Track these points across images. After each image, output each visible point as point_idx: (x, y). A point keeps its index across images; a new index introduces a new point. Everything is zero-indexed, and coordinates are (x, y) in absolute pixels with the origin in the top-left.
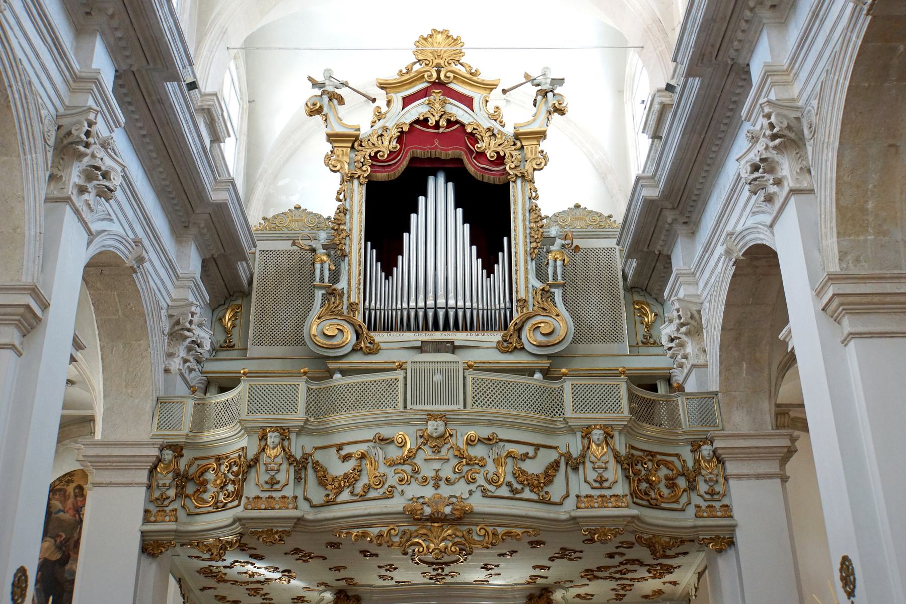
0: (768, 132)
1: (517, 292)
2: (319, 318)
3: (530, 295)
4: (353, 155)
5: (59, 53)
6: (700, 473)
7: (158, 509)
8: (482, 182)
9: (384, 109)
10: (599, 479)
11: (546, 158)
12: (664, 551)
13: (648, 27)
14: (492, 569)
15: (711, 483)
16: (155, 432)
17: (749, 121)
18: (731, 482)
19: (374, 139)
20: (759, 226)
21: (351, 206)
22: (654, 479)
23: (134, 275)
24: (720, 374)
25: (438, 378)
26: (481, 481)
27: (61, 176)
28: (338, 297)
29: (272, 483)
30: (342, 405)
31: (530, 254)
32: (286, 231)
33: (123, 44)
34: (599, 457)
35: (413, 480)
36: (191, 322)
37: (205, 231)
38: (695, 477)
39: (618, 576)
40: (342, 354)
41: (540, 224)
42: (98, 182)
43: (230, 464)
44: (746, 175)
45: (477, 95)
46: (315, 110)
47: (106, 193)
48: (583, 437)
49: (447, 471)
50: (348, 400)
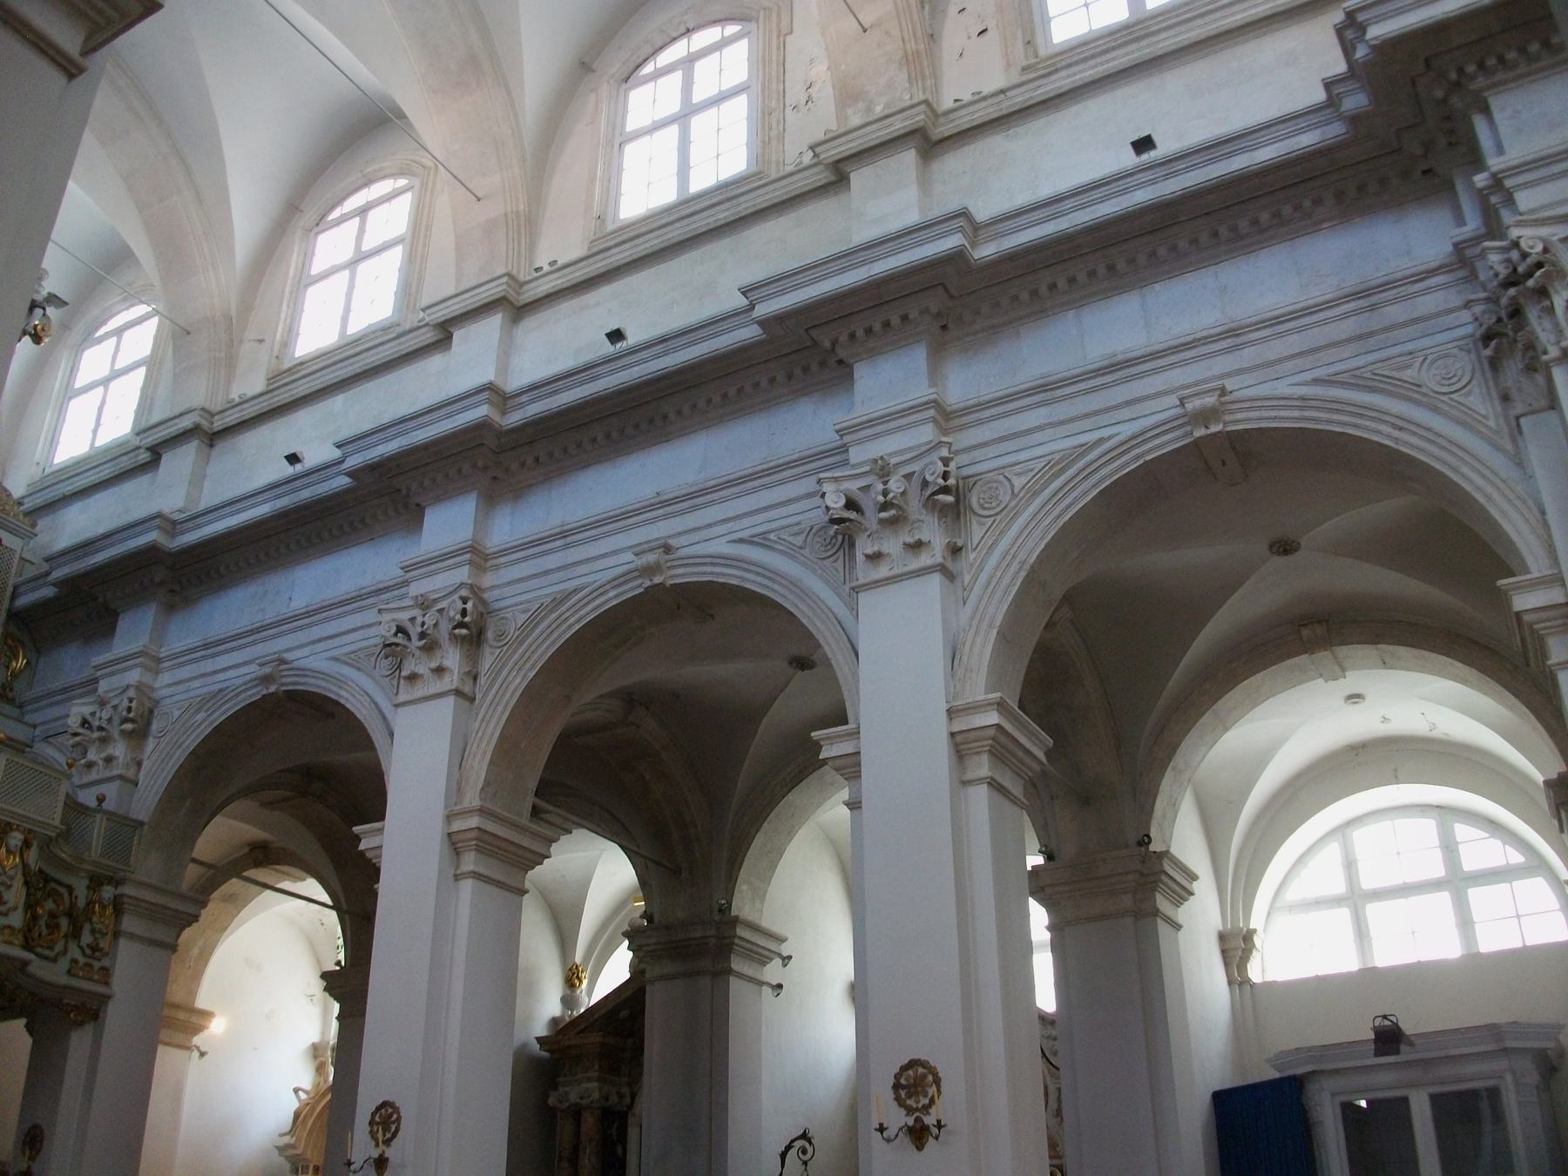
15: (98, 936)
18: (122, 942)
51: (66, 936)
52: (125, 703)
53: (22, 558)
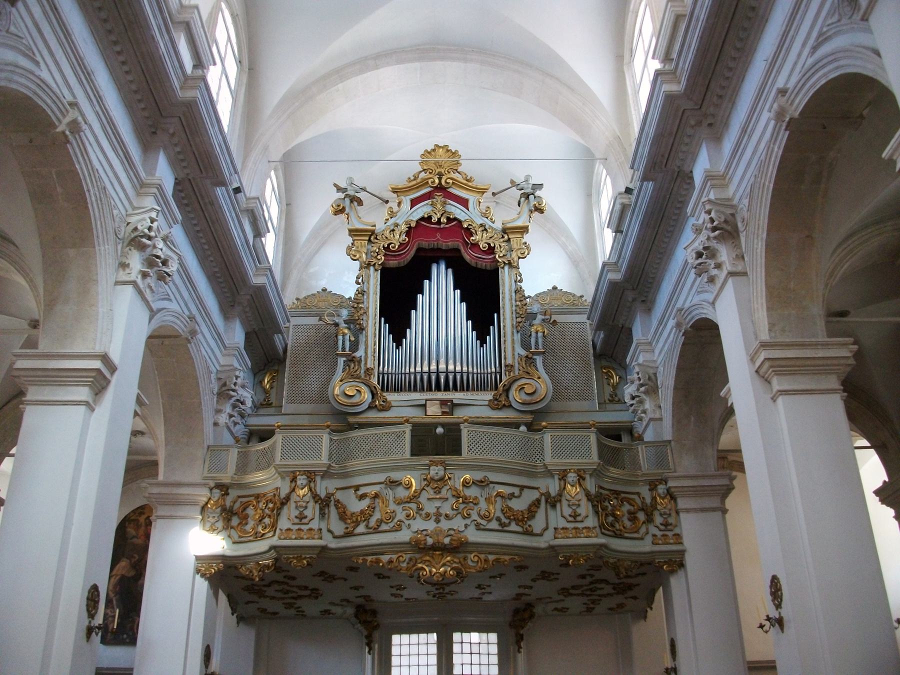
0: (709, 225)
1: (505, 358)
2: (341, 381)
3: (516, 361)
5: (129, 164)
6: (656, 508)
9: (396, 208)
10: (573, 514)
11: (528, 248)
12: (626, 573)
13: (610, 143)
14: (484, 588)
16: (206, 474)
17: (693, 217)
18: (682, 515)
19: (387, 233)
20: (704, 303)
21: (368, 289)
22: (618, 513)
23: (189, 345)
25: (440, 430)
26: (475, 516)
27: (129, 264)
28: (357, 363)
29: (301, 517)
32: (315, 309)
33: (181, 157)
34: (573, 496)
35: (418, 516)
36: (235, 384)
37: (247, 309)
38: (652, 511)
39: (588, 593)
41: (524, 303)
42: (159, 269)
43: (267, 501)
44: (692, 260)
45: (472, 198)
46: (339, 211)
47: (162, 277)
48: (560, 479)
49: (446, 509)
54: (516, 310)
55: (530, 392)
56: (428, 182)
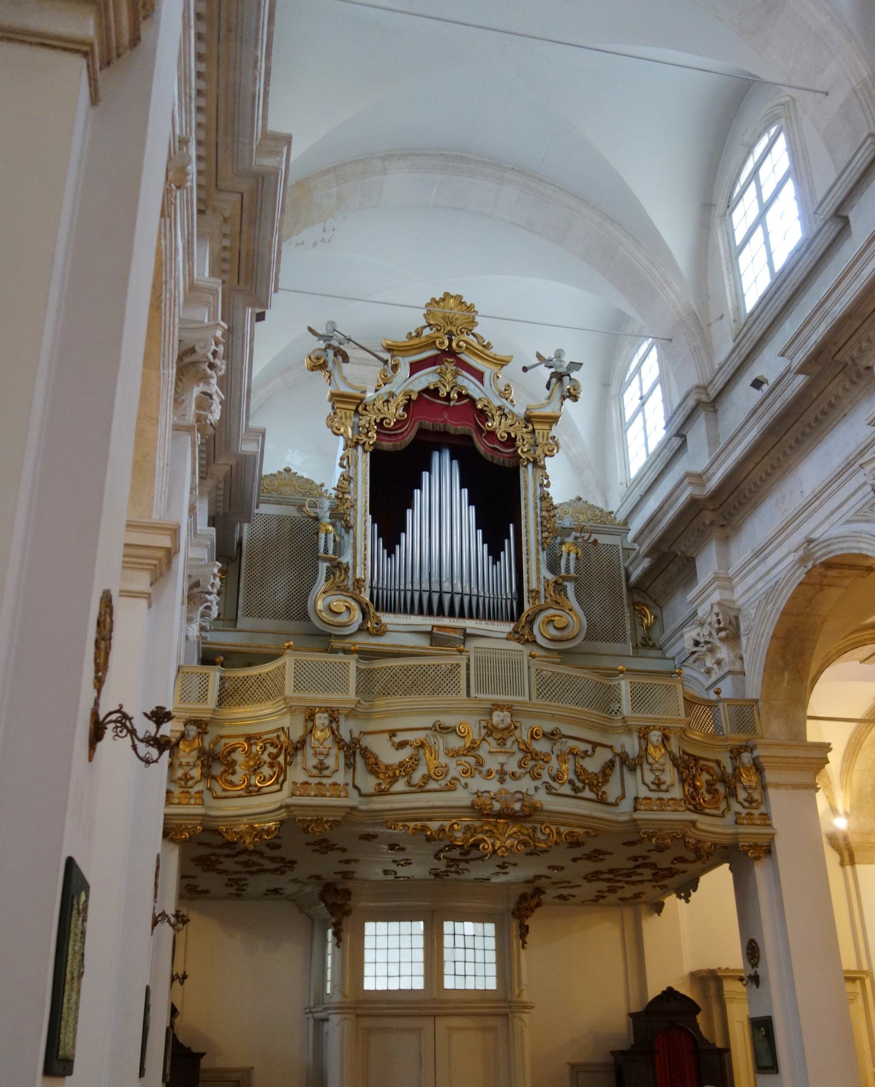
1: (528, 582)
2: (325, 592)
4: (356, 420)
7: (181, 790)
8: (492, 464)
11: (557, 444)
15: (749, 791)
18: (771, 791)
21: (356, 474)
24: (763, 682)
26: (546, 778)
28: (343, 571)
29: (321, 767)
30: (396, 688)
31: (542, 544)
32: (275, 494)
35: (477, 773)
40: (348, 633)
41: (552, 514)
48: (639, 737)
49: (512, 766)
50: (403, 683)
51: (726, 797)
52: (715, 618)
53: (624, 549)
54: (542, 523)
55: (561, 626)
56: (435, 342)
